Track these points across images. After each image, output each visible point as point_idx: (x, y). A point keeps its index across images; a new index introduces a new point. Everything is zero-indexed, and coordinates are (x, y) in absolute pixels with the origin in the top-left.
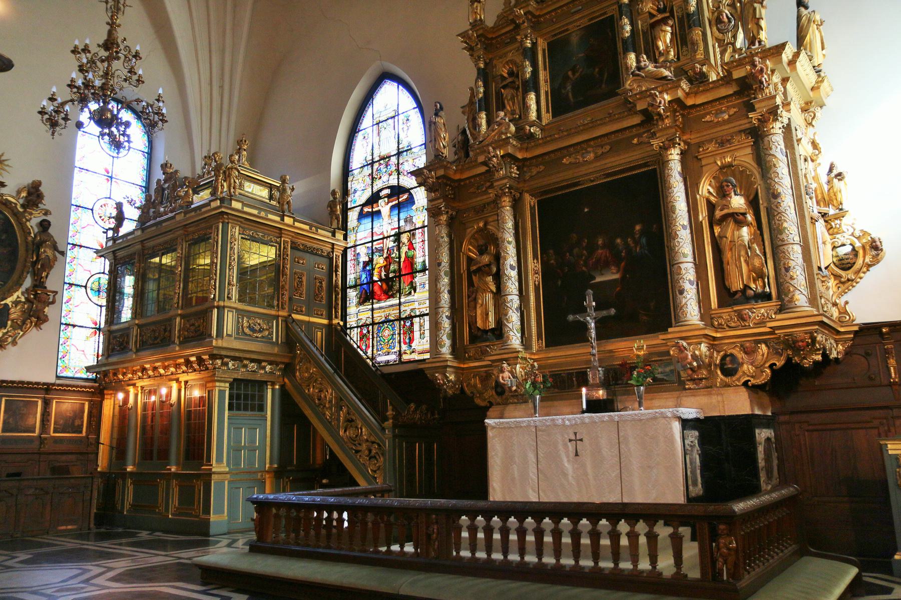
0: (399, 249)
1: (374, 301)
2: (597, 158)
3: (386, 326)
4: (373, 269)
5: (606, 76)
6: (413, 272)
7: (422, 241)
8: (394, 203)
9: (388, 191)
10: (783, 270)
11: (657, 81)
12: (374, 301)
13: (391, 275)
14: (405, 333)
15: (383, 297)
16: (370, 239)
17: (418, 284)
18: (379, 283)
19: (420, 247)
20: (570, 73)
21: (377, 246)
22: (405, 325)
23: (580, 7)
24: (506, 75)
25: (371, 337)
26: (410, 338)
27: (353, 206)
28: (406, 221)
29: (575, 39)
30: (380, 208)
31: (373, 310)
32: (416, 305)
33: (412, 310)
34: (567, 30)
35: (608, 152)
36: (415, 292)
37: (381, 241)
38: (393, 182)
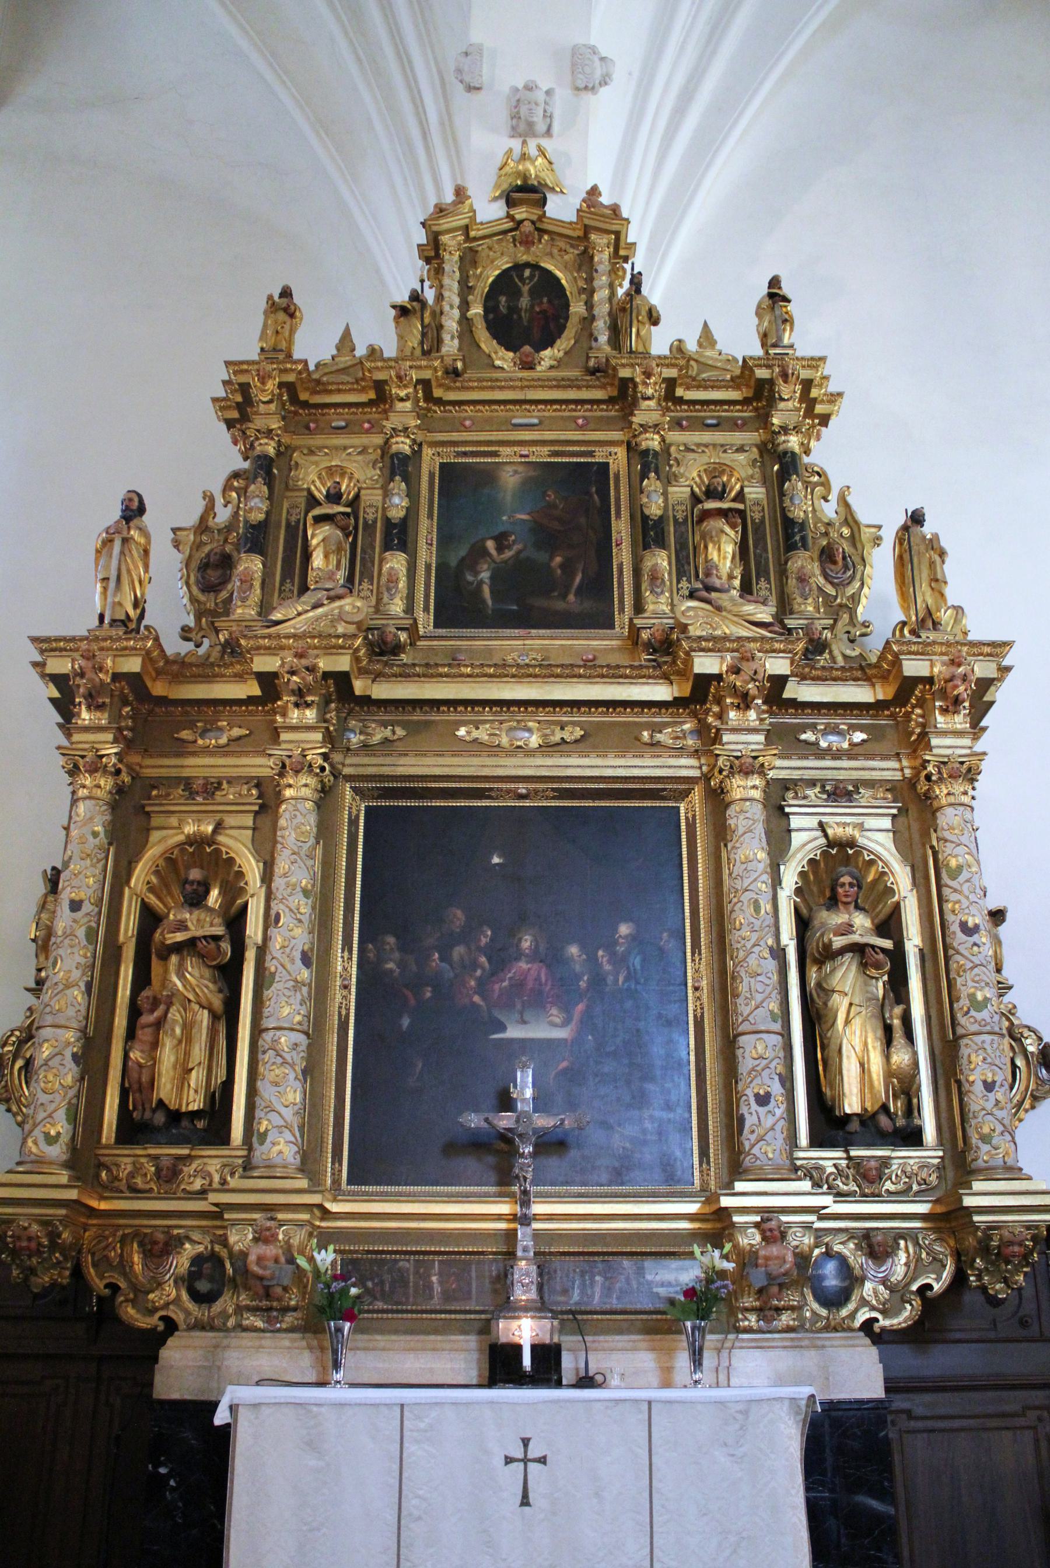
2: (548, 748)
5: (578, 579)
10: (979, 1087)
11: (747, 624)
20: (490, 544)
23: (536, 421)
24: (319, 496)
29: (510, 480)
34: (495, 454)
35: (576, 741)
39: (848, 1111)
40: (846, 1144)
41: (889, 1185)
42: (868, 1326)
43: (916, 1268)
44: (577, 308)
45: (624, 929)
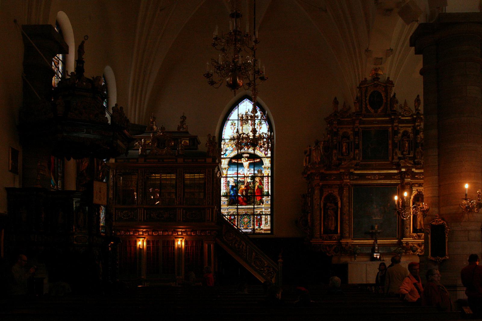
0: (254, 182)
1: (238, 205)
3: (246, 217)
4: (239, 190)
6: (262, 195)
7: (267, 182)
8: (251, 161)
12: (238, 205)
13: (249, 195)
14: (257, 221)
15: (244, 204)
16: (236, 176)
17: (264, 201)
18: (242, 197)
19: (266, 185)
21: (241, 180)
22: (257, 218)
25: (236, 220)
26: (259, 224)
27: (225, 157)
28: (258, 171)
30: (242, 162)
32: (263, 210)
36: (263, 204)
37: (243, 178)
38: (251, 151)
39: (418, 228)
40: (417, 233)
41: (422, 238)
42: (418, 254)
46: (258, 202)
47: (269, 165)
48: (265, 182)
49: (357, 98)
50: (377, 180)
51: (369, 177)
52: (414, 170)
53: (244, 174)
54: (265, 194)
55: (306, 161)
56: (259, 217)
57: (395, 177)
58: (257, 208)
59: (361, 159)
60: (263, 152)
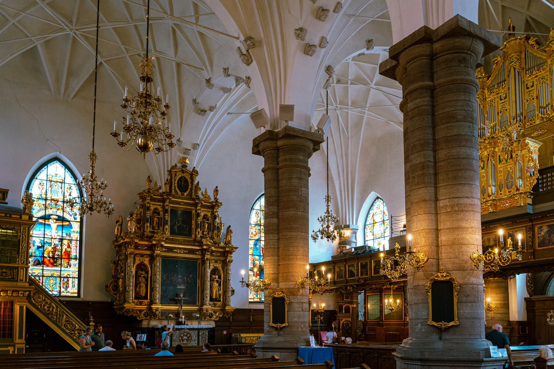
0: (62, 246)
9: (57, 217)
12: (44, 266)
13: (56, 256)
14: (63, 284)
18: (48, 258)
21: (47, 241)
26: (66, 286)
28: (67, 234)
31: (43, 270)
32: (71, 273)
33: (68, 274)
36: (70, 266)
37: (51, 239)
38: (60, 213)
40: (213, 301)
42: (214, 320)
43: (219, 314)
44: (190, 187)
45: (191, 276)
46: (66, 264)
47: (79, 230)
48: (73, 245)
49: (167, 180)
50: (182, 254)
51: (176, 251)
52: (213, 248)
53: (51, 236)
54: (73, 257)
55: (118, 229)
56: (66, 280)
57: (197, 253)
58: (64, 270)
59: (169, 233)
60: (73, 216)
